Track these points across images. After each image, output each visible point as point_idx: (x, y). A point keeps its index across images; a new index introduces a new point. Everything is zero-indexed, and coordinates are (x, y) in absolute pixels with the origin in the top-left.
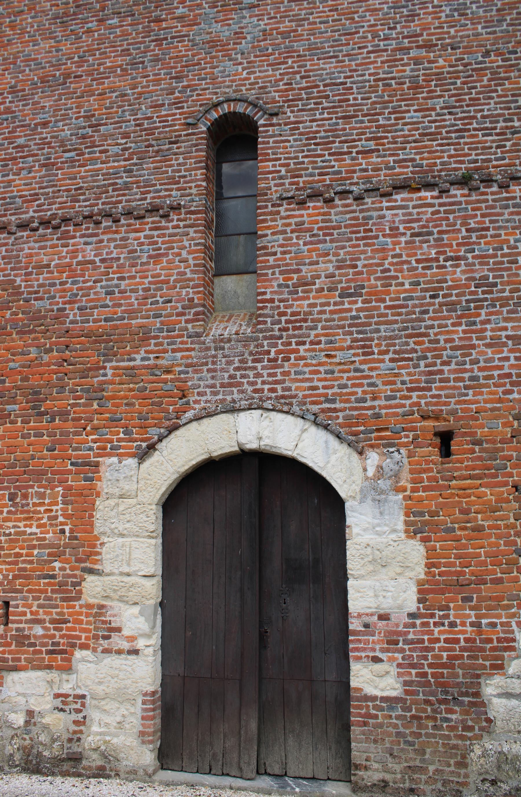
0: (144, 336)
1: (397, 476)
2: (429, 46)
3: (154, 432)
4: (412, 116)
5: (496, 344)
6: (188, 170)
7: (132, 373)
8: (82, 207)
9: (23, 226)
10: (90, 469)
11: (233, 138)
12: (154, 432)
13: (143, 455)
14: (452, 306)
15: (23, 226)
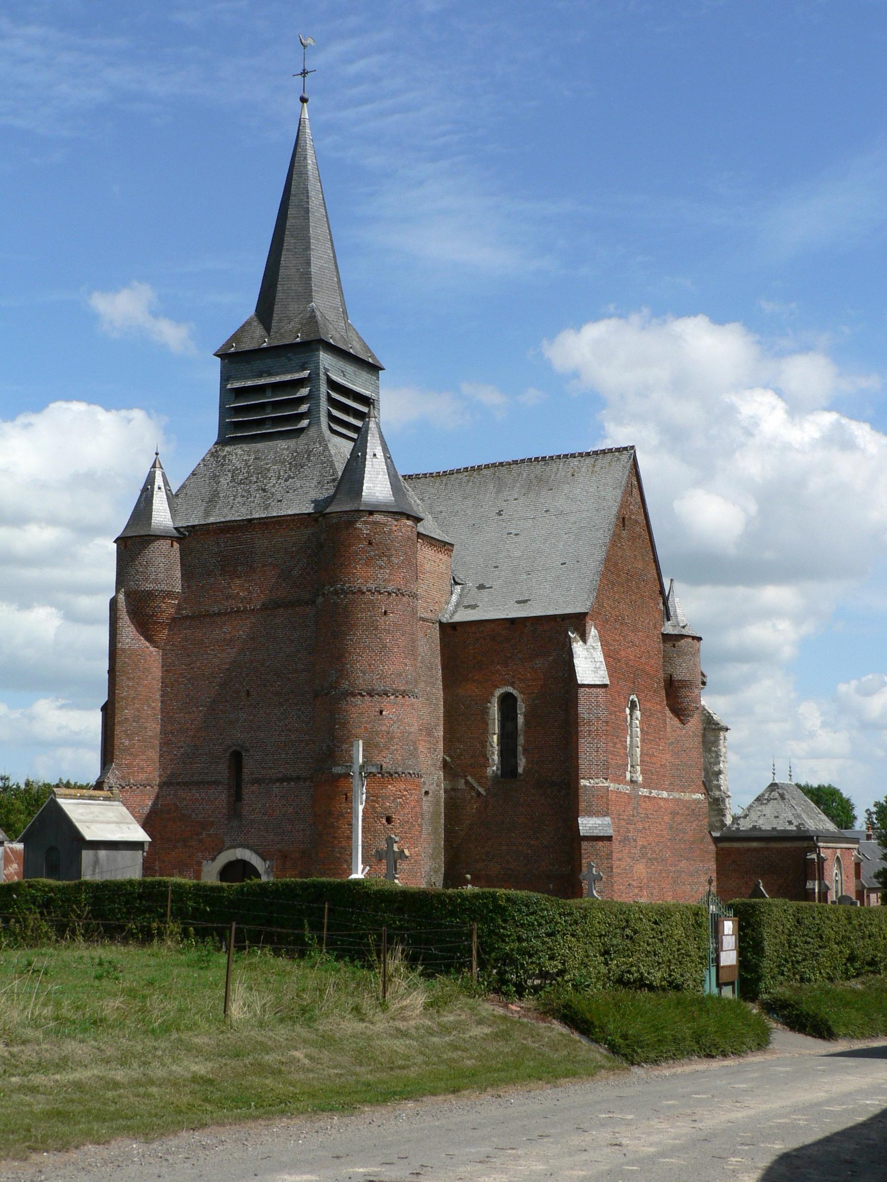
0: (212, 824)
1: (272, 868)
2: (289, 730)
3: (215, 853)
4: (283, 756)
5: (298, 831)
6: (223, 770)
7: (209, 835)
8: (195, 778)
9: (178, 784)
10: (199, 864)
11: (236, 759)
12: (215, 853)
13: (213, 859)
14: (288, 819)
15: (178, 784)
